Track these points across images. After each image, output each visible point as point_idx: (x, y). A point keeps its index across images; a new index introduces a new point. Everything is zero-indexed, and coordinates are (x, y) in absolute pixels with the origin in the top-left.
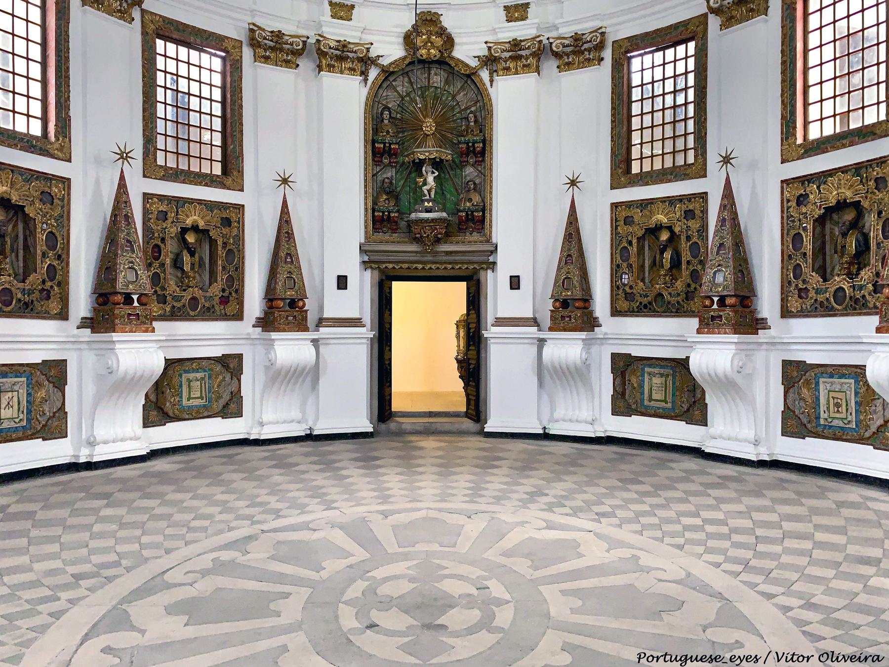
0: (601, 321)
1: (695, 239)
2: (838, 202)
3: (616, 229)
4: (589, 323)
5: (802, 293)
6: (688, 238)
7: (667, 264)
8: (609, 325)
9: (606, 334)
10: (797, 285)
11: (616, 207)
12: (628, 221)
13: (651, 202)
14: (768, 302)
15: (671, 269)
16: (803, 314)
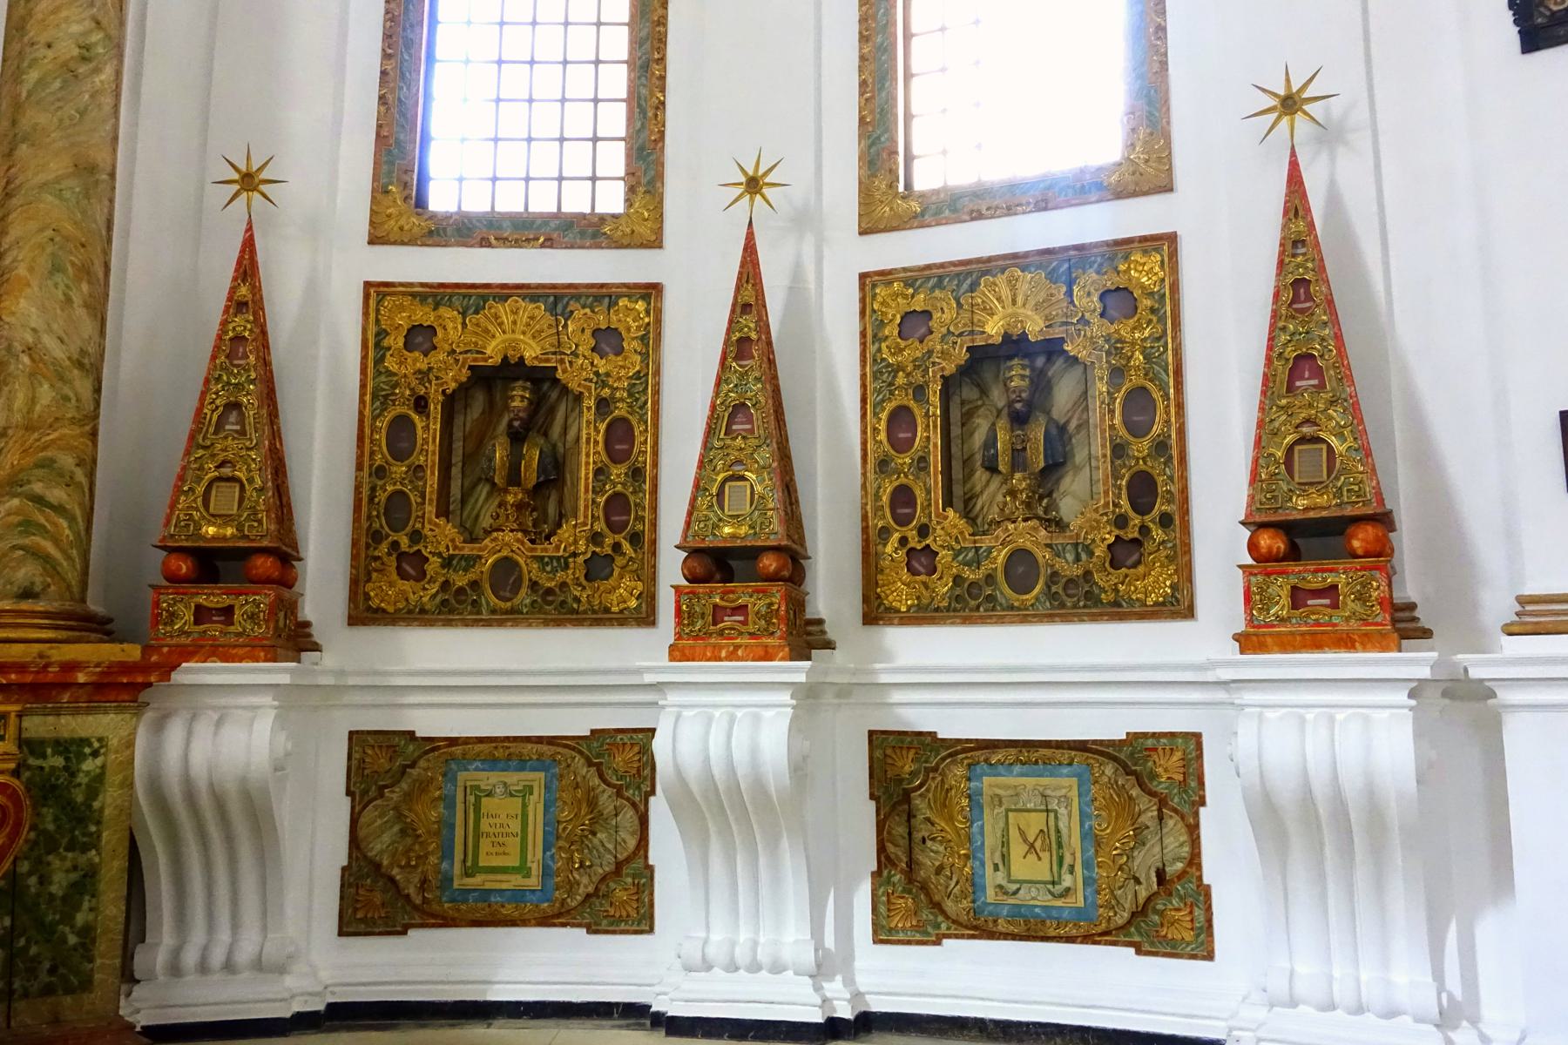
0: (317, 634)
1: (621, 410)
2: (1007, 337)
3: (379, 361)
4: (295, 639)
5: (921, 559)
6: (603, 405)
7: (530, 476)
8: (345, 652)
9: (341, 673)
10: (903, 541)
11: (382, 297)
12: (421, 338)
13: (503, 292)
14: (831, 588)
15: (538, 487)
16: (925, 614)
